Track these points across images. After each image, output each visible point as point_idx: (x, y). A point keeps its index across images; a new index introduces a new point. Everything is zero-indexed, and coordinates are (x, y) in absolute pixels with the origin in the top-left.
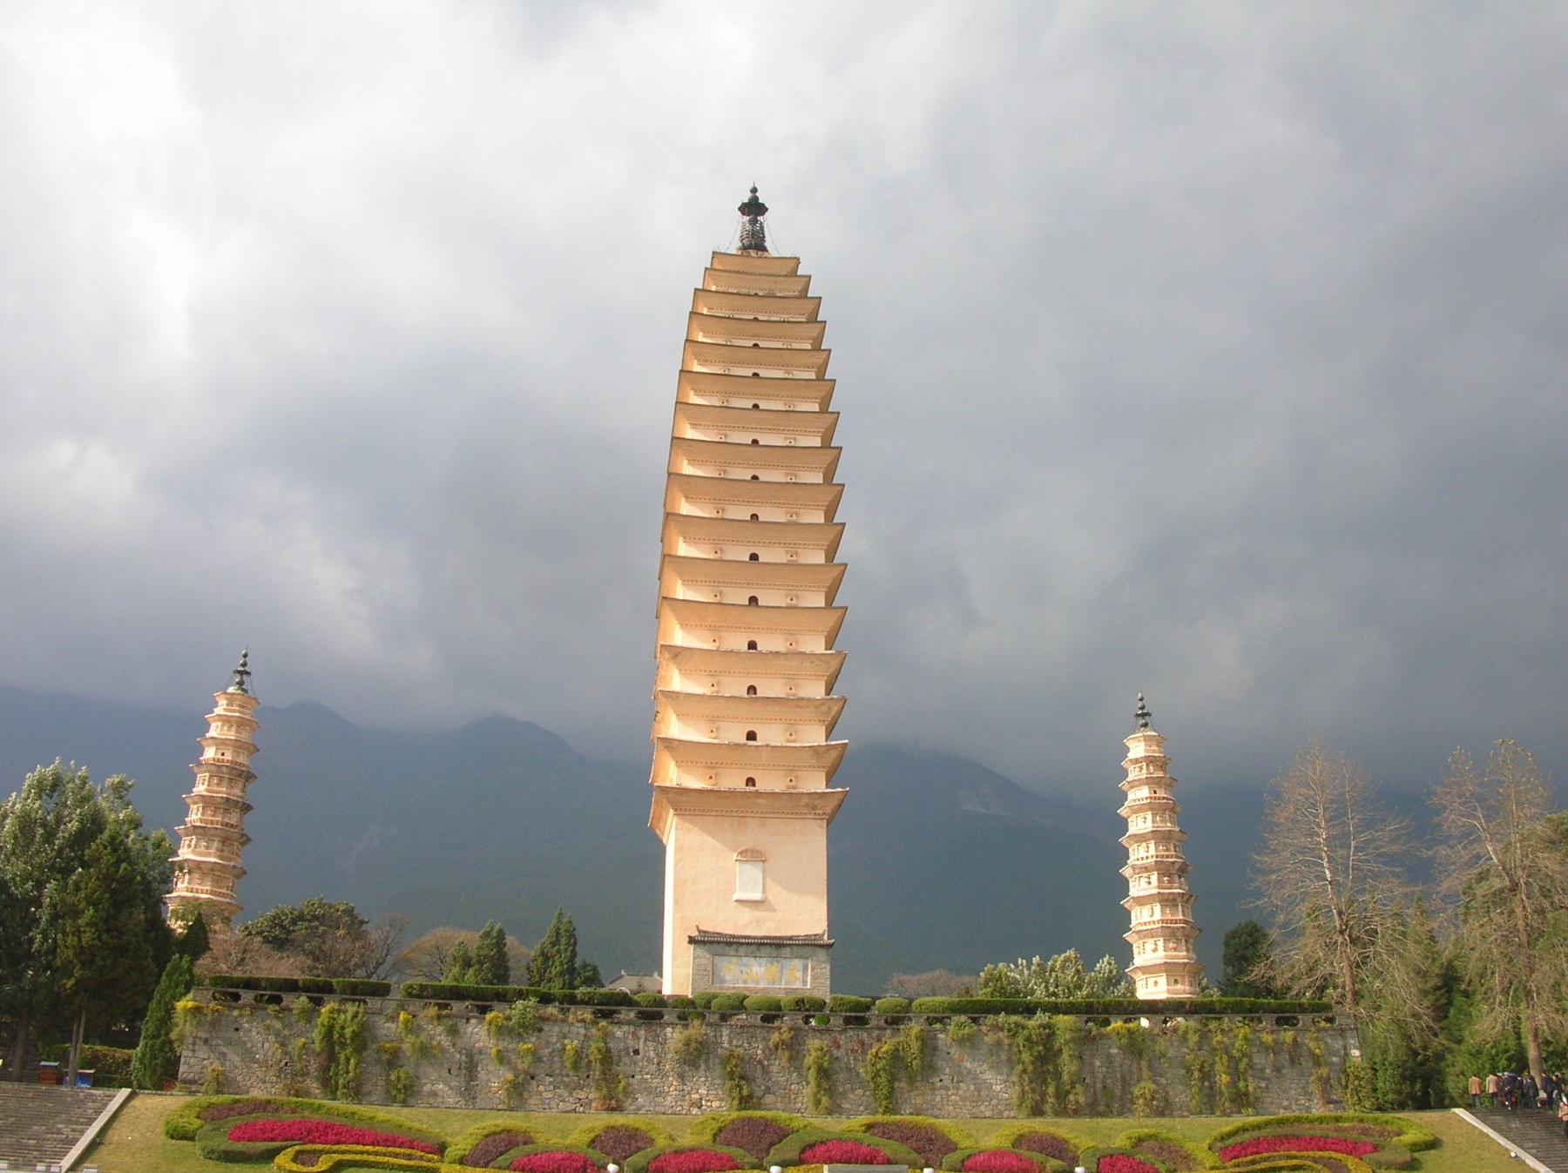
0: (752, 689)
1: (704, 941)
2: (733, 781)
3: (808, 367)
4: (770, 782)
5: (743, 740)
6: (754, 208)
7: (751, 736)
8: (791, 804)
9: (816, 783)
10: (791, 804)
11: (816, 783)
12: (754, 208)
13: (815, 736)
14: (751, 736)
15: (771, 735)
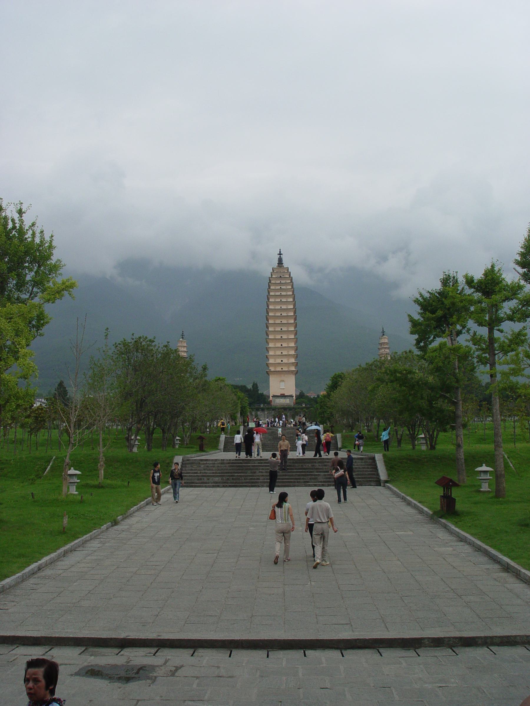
0: (282, 353)
1: (274, 396)
2: (279, 369)
3: (290, 291)
4: (285, 369)
5: (280, 362)
6: (280, 254)
7: (282, 361)
8: (289, 372)
9: (293, 368)
10: (289, 372)
11: (293, 368)
12: (280, 254)
13: (293, 360)
14: (282, 361)
15: (285, 361)
